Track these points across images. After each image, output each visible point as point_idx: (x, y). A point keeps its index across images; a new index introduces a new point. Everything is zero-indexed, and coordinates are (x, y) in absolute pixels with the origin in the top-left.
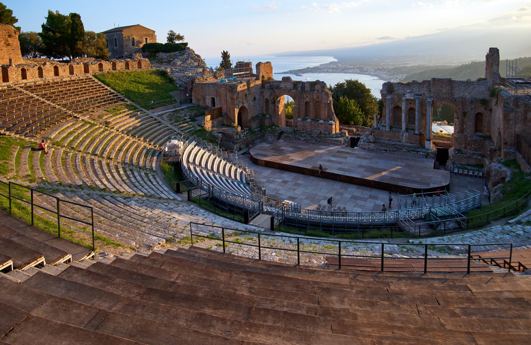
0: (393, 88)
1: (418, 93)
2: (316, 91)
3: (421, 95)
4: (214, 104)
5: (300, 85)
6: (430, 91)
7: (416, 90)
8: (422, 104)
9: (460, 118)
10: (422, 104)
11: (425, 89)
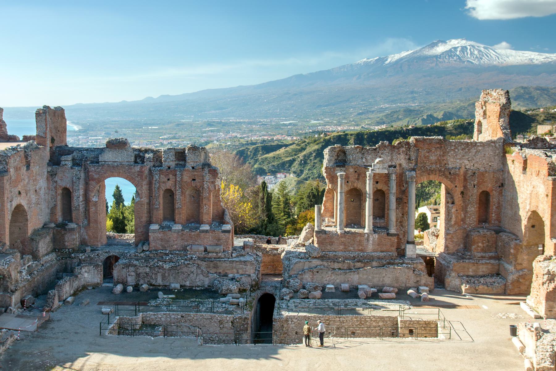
1: (390, 163)
6: (409, 159)
11: (402, 156)
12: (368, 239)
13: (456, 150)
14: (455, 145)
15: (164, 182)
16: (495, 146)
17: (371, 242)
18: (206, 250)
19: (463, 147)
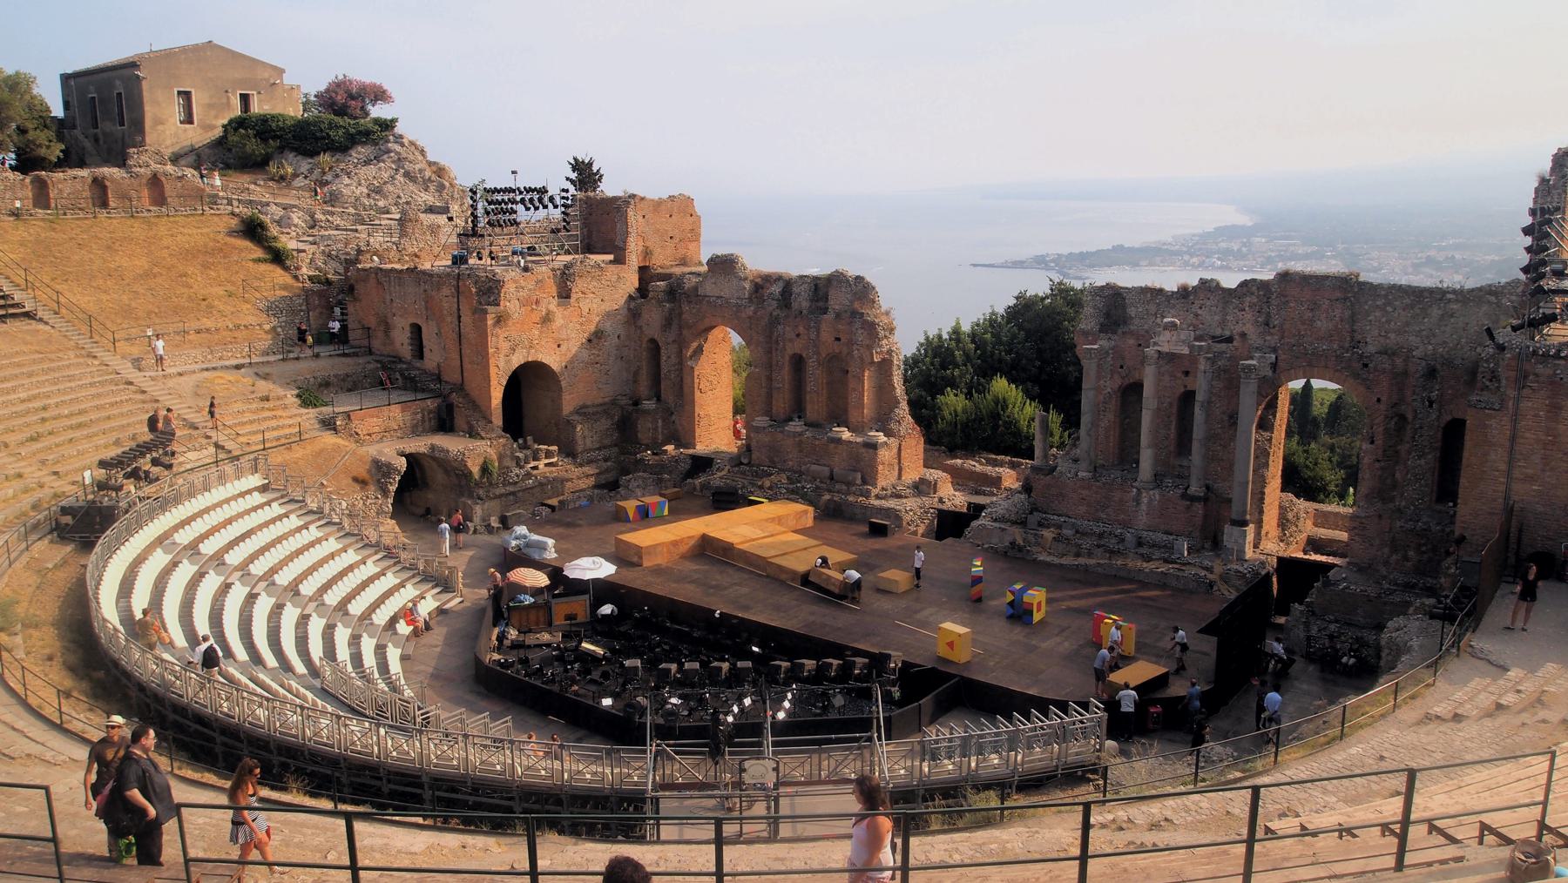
0: (1124, 307)
1: (1218, 332)
2: (830, 316)
3: (1229, 340)
4: (419, 351)
5: (776, 289)
7: (1210, 318)
8: (1229, 378)
9: (1379, 441)
10: (1229, 378)
11: (1248, 316)
12: (1137, 500)
13: (1389, 309)
14: (1386, 296)
15: (791, 340)
16: (1499, 305)
17: (1144, 507)
18: (832, 478)
19: (1407, 301)
